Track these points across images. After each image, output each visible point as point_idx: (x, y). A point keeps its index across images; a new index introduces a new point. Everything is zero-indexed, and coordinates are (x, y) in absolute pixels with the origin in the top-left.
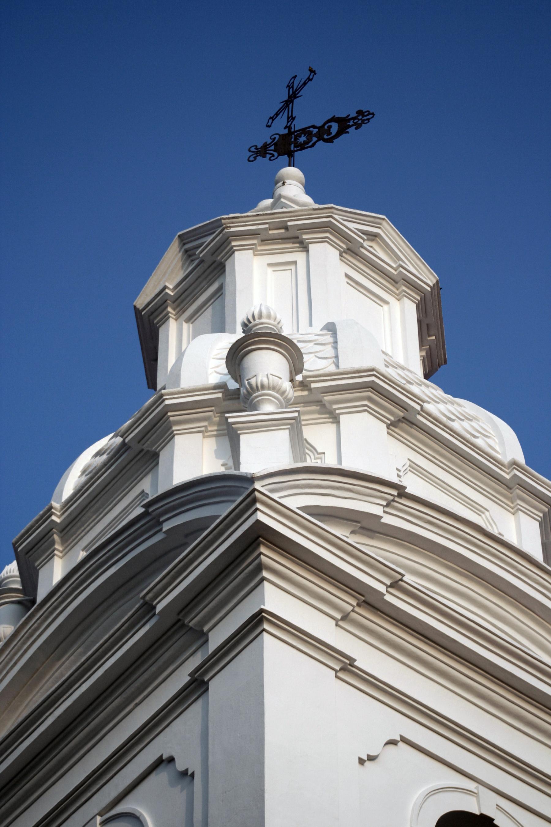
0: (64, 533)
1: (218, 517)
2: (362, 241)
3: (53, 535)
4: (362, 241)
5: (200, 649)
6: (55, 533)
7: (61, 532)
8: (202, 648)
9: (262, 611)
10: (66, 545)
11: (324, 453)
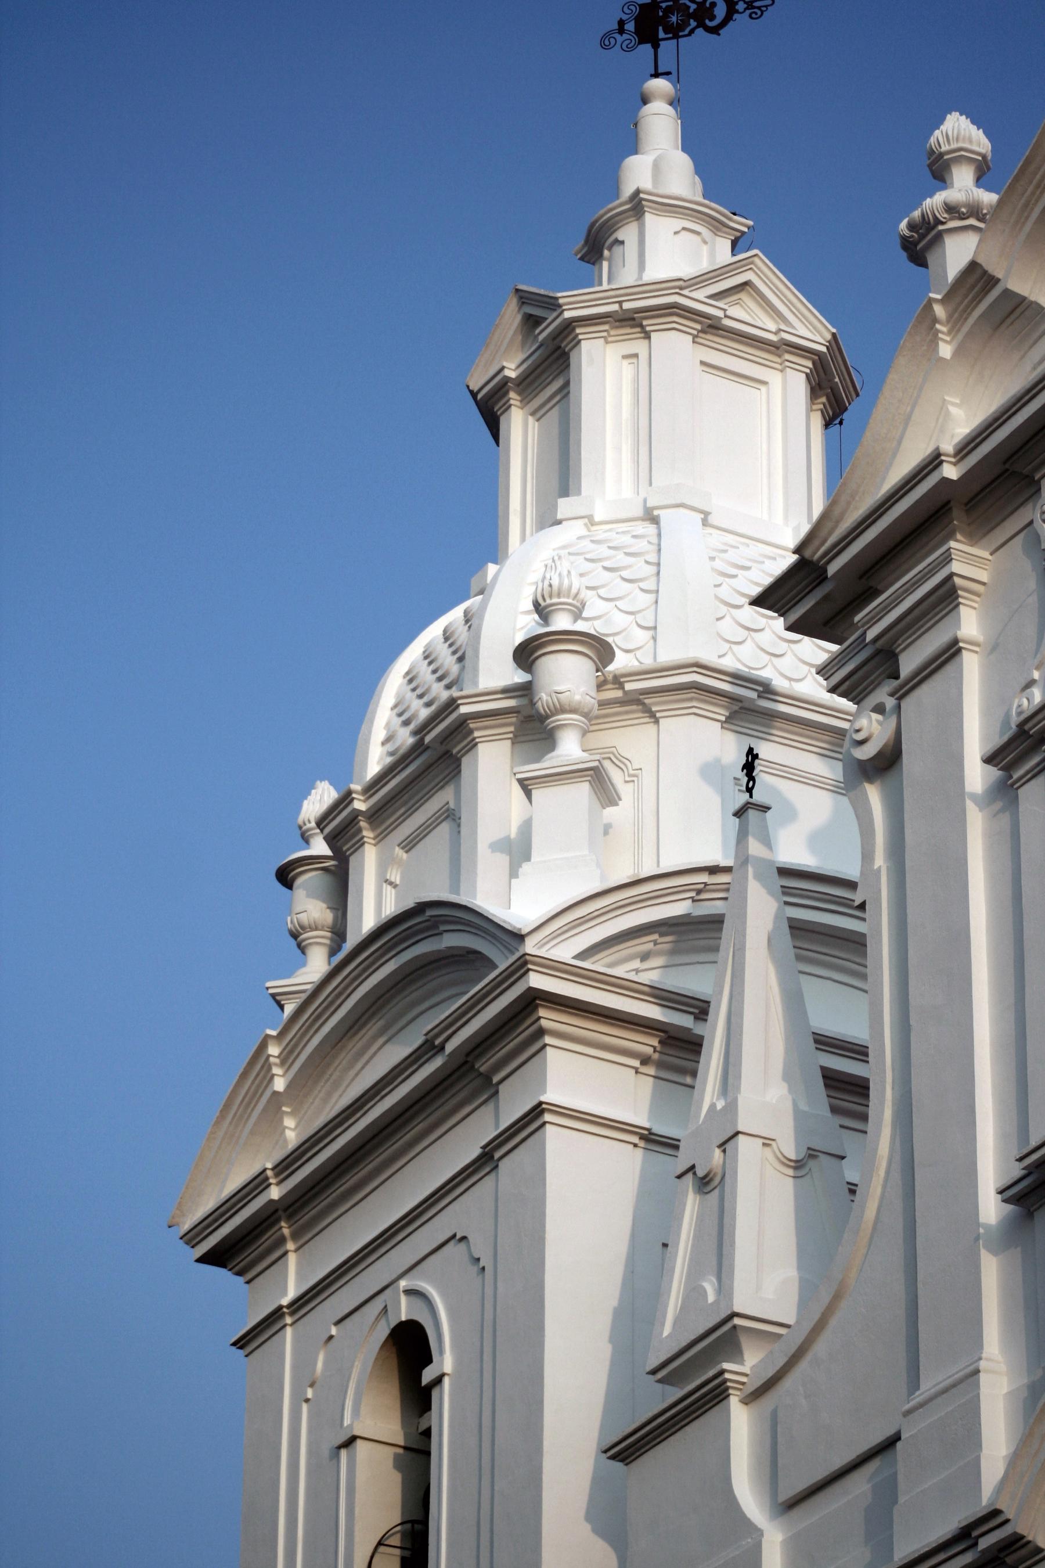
0: (372, 820)
5: (491, 1100)
6: (360, 820)
10: (379, 830)
11: (641, 769)
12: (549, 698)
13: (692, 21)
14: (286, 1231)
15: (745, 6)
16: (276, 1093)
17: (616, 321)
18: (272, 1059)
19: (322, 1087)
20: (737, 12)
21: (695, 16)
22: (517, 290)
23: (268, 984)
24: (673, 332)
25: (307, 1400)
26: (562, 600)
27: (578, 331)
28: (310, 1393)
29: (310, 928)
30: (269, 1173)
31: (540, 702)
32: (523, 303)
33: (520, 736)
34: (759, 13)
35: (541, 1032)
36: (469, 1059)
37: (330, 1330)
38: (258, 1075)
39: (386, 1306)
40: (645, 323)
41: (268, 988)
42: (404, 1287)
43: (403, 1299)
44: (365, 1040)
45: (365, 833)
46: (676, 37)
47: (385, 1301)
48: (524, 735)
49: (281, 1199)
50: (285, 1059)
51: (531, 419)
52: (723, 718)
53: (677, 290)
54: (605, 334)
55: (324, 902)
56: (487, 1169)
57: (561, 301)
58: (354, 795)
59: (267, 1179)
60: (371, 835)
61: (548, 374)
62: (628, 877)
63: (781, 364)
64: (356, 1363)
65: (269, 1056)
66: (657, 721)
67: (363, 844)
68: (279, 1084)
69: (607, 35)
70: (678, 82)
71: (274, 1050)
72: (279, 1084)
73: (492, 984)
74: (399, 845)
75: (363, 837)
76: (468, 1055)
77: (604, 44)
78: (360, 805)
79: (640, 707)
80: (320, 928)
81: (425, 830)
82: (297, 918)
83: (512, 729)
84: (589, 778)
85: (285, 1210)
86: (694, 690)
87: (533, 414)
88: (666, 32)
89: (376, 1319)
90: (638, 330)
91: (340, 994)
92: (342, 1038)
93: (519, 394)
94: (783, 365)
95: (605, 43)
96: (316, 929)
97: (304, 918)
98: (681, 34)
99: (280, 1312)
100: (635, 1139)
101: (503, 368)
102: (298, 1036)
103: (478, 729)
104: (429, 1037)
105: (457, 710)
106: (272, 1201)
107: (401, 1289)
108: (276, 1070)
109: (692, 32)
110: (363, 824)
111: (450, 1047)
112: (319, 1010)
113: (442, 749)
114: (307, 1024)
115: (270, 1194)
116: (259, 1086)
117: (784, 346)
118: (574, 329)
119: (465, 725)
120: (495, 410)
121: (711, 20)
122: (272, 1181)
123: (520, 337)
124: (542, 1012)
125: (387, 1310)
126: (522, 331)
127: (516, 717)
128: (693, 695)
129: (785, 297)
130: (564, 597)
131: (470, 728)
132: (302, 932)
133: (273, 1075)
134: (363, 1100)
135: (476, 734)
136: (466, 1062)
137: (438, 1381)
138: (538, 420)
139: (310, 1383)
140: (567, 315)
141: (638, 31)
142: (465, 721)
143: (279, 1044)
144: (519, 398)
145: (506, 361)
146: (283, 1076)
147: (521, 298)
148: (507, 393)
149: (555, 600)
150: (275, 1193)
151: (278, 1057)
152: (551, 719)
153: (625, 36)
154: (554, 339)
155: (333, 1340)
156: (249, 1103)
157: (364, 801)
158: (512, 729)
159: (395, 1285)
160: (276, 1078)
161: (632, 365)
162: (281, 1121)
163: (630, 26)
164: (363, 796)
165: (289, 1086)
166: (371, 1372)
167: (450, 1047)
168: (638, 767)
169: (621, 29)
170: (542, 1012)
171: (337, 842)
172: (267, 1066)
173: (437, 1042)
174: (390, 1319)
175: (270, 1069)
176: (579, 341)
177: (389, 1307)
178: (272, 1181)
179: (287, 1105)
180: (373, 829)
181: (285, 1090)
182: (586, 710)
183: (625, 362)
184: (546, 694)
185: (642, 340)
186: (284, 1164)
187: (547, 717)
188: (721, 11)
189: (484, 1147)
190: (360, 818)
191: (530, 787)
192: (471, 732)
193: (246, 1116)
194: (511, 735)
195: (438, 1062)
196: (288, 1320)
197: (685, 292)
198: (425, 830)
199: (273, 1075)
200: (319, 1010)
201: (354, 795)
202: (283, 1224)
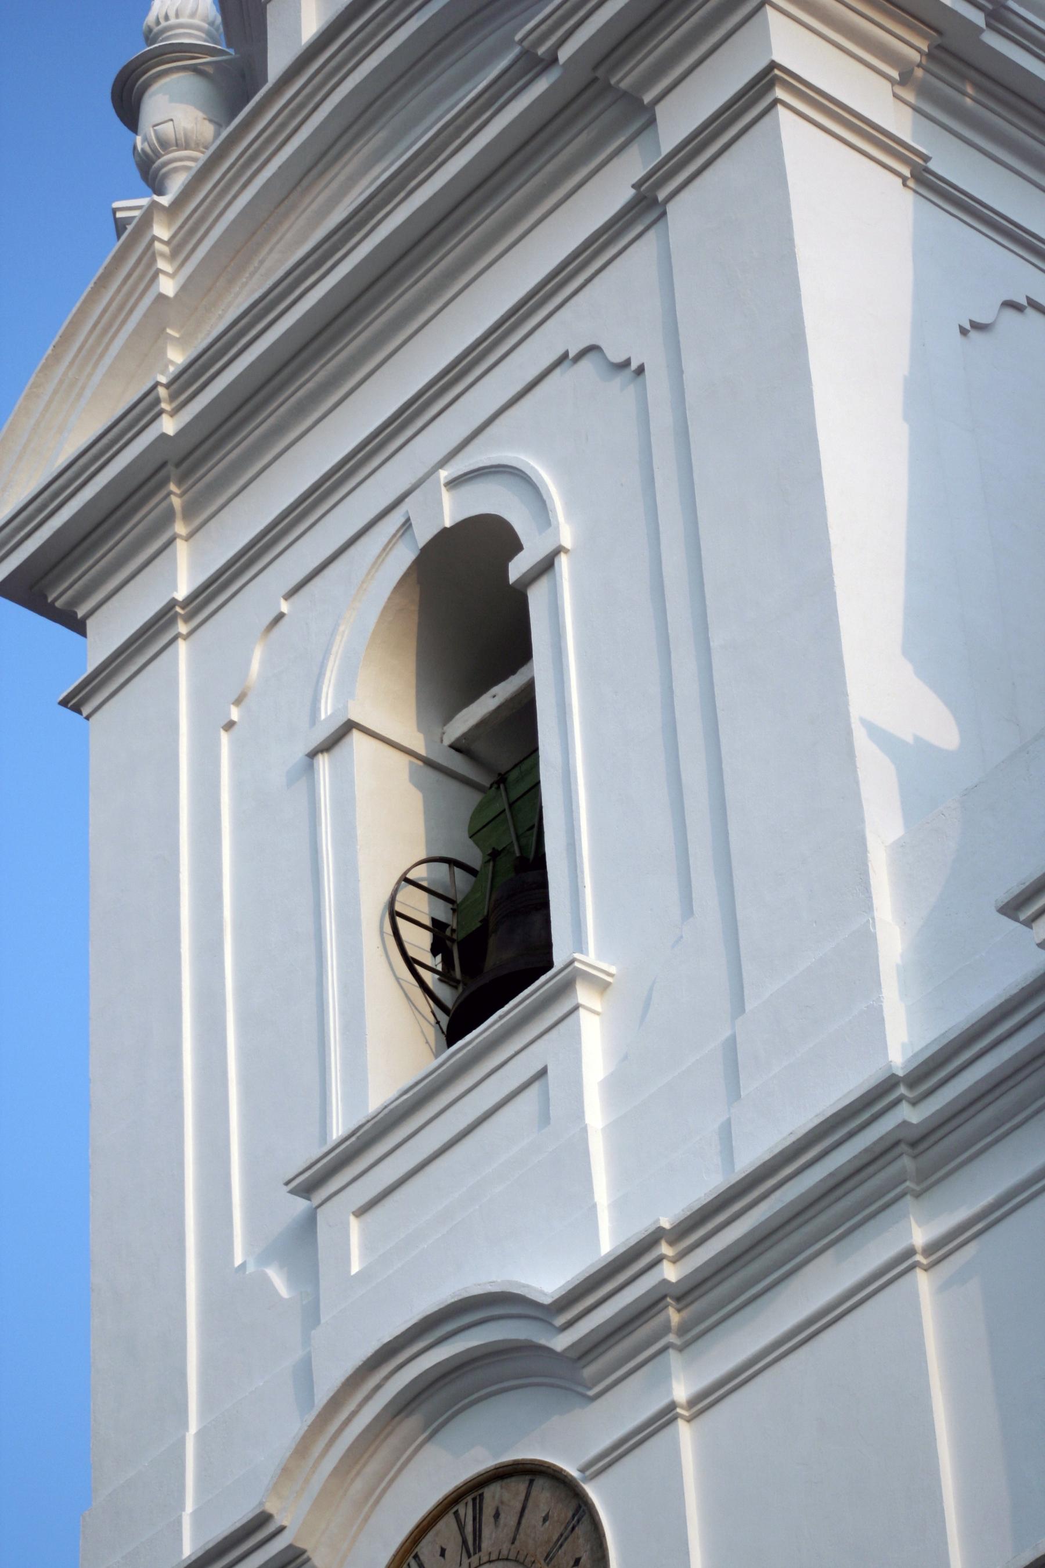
8: (639, 139)
9: (773, 65)
14: (176, 502)
16: (161, 297)
18: (157, 245)
23: (116, 205)
25: (230, 725)
28: (235, 714)
29: (177, 145)
30: (162, 392)
36: (600, 73)
37: (279, 604)
38: (129, 275)
39: (408, 520)
41: (114, 211)
42: (446, 477)
43: (446, 496)
44: (335, 185)
47: (407, 512)
49: (181, 433)
50: (178, 248)
56: (639, 228)
59: (158, 401)
64: (341, 628)
65: (155, 238)
68: (168, 286)
71: (161, 231)
72: (168, 286)
76: (596, 67)
80: (193, 145)
82: (155, 131)
85: (178, 465)
89: (384, 549)
97: (167, 129)
99: (172, 613)
100: (906, 172)
102: (212, 197)
104: (526, 44)
106: (163, 436)
107: (443, 481)
108: (162, 264)
111: (564, 54)
112: (255, 146)
116: (130, 294)
122: (164, 405)
125: (411, 525)
132: (163, 153)
133: (159, 271)
136: (595, 80)
137: (547, 566)
139: (235, 697)
143: (169, 225)
146: (172, 276)
150: (169, 426)
151: (167, 243)
155: (284, 623)
156: (105, 331)
159: (432, 478)
160: (162, 278)
162: (163, 352)
165: (183, 289)
167: (564, 54)
172: (149, 256)
173: (541, 51)
175: (153, 260)
178: (164, 405)
179: (172, 328)
181: (176, 295)
186: (186, 376)
193: (99, 351)
195: (541, 86)
196: (182, 628)
200: (255, 146)
202: (172, 487)
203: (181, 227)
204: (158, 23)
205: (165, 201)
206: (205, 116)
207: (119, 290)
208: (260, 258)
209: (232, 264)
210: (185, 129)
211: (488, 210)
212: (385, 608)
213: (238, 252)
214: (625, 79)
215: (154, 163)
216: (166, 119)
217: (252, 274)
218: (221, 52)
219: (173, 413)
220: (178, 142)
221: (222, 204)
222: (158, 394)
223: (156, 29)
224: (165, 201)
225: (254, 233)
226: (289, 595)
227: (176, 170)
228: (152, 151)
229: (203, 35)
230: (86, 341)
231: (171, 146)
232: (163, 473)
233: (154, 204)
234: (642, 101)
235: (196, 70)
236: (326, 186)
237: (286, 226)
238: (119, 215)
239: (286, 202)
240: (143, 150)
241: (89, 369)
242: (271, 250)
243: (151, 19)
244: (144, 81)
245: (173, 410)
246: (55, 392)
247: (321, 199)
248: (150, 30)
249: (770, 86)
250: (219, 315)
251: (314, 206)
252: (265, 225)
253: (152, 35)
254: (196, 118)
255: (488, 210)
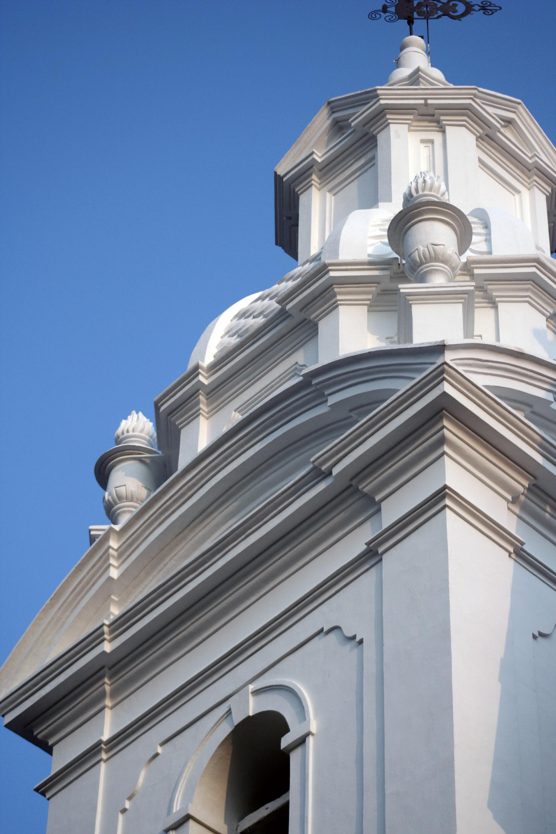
1: (396, 391)
2: (499, 126)
3: (198, 396)
4: (499, 126)
6: (200, 394)
7: (208, 394)
9: (445, 487)
12: (426, 249)
13: (439, 12)
14: (107, 688)
15: (480, 8)
16: (110, 579)
17: (419, 115)
18: (111, 551)
19: (155, 576)
20: (474, 10)
21: (441, 9)
22: (329, 103)
23: (91, 527)
24: (464, 128)
25: (124, 811)
26: (432, 193)
27: (388, 116)
28: (127, 805)
29: (126, 499)
30: (106, 629)
31: (417, 252)
32: (333, 112)
33: (373, 306)
34: (491, 12)
35: (443, 441)
36: (354, 482)
37: (157, 749)
39: (230, 710)
40: (442, 118)
41: (90, 531)
42: (252, 689)
43: (251, 699)
44: (208, 528)
45: (201, 406)
46: (427, 18)
47: (230, 705)
48: (376, 306)
49: (113, 652)
50: (122, 554)
51: (328, 195)
52: (548, 314)
53: (472, 96)
54: (409, 122)
55: (141, 481)
57: (379, 92)
58: (200, 370)
59: (103, 633)
60: (206, 410)
61: (350, 158)
62: (517, 348)
63: (529, 184)
64: (189, 764)
65: (110, 547)
66: (494, 305)
67: (198, 415)
68: (114, 573)
69: (375, 12)
70: (428, 43)
71: (114, 543)
72: (114, 573)
73: (397, 401)
74: (235, 411)
75: (200, 409)
76: (352, 479)
77: (371, 16)
78: (204, 379)
79: (482, 293)
80: (135, 500)
81: (266, 392)
82: (116, 491)
83: (370, 297)
84: (463, 301)
85: (110, 669)
86: (531, 282)
87: (330, 191)
88: (418, 14)
89: (216, 724)
90: (435, 124)
91: (194, 485)
92: (184, 530)
93: (319, 179)
94: (532, 184)
95: (373, 16)
96: (132, 500)
97: (122, 491)
98: (430, 17)
100: (511, 549)
101: (313, 153)
103: (341, 294)
104: (316, 463)
105: (328, 274)
106: (104, 653)
107: (250, 691)
108: (112, 561)
109: (439, 17)
110: (201, 397)
111: (336, 471)
113: (303, 315)
114: (153, 518)
115: (103, 647)
117: (535, 169)
118: (385, 115)
119: (330, 289)
120: (296, 190)
121: (453, 12)
123: (326, 138)
124: (446, 423)
125: (231, 713)
126: (328, 133)
127: (376, 287)
128: (529, 286)
129: (538, 137)
130: (434, 192)
131: (334, 291)
132: (119, 502)
133: (110, 565)
134: (225, 541)
135: (339, 297)
136: (351, 486)
137: (302, 741)
138: (334, 195)
139: (129, 795)
140: (382, 102)
141: (397, 12)
142: (332, 285)
143: (119, 539)
144: (319, 181)
145: (316, 149)
146: (117, 568)
147: (332, 109)
148: (311, 175)
149: (426, 192)
150: (107, 647)
151: (116, 550)
152: (426, 265)
153: (387, 14)
154: (364, 126)
156: (79, 594)
157: (207, 378)
158: (370, 297)
159: (244, 689)
160: (112, 569)
161: (428, 148)
162: (108, 608)
163: (393, 9)
164: (207, 374)
165: (122, 576)
166: (206, 768)
167: (336, 471)
168: (479, 334)
169: (385, 9)
170: (446, 423)
171: (172, 417)
172: (106, 556)
173: (323, 468)
174: (234, 718)
175: (108, 559)
176: (389, 124)
177: (232, 710)
178: (106, 636)
180: (208, 405)
181: (118, 578)
182: (454, 265)
183: (422, 146)
184: (423, 246)
185: (436, 133)
186: (119, 622)
187: (422, 264)
188: (461, 8)
189: (368, 544)
190: (200, 391)
191: (410, 302)
192: (335, 296)
194: (368, 302)
195: (322, 486)
196: (104, 756)
197: (478, 100)
198: (266, 392)
199: (110, 565)
201: (200, 370)
202: (106, 680)
203: (124, 543)
204: (123, 434)
205: (117, 528)
206: (142, 485)
207: (88, 573)
208: (165, 563)
209: (150, 565)
210: (131, 491)
211: (288, 549)
212: (213, 756)
213: (153, 558)
214: (366, 487)
215: (113, 507)
216: (123, 484)
217: (160, 571)
218: (155, 452)
219: (111, 641)
220: (128, 497)
221: (147, 532)
222: (103, 630)
223: (121, 437)
224: (117, 528)
225: (163, 549)
226: (163, 744)
227: (124, 512)
228: (113, 501)
229: (146, 442)
230: (68, 597)
231: (123, 499)
232: (102, 672)
233: (111, 529)
234: (375, 499)
235: (140, 460)
236: (203, 528)
237: (180, 547)
238: (92, 533)
239: (181, 535)
240: (108, 500)
241: (68, 613)
242: (171, 559)
243: (119, 431)
244: (114, 463)
245: (110, 639)
246: (49, 623)
247: (201, 534)
248: (118, 437)
249: (443, 498)
250: (140, 591)
251: (196, 538)
252: (169, 546)
253: (119, 440)
254: (138, 486)
255: (288, 549)
